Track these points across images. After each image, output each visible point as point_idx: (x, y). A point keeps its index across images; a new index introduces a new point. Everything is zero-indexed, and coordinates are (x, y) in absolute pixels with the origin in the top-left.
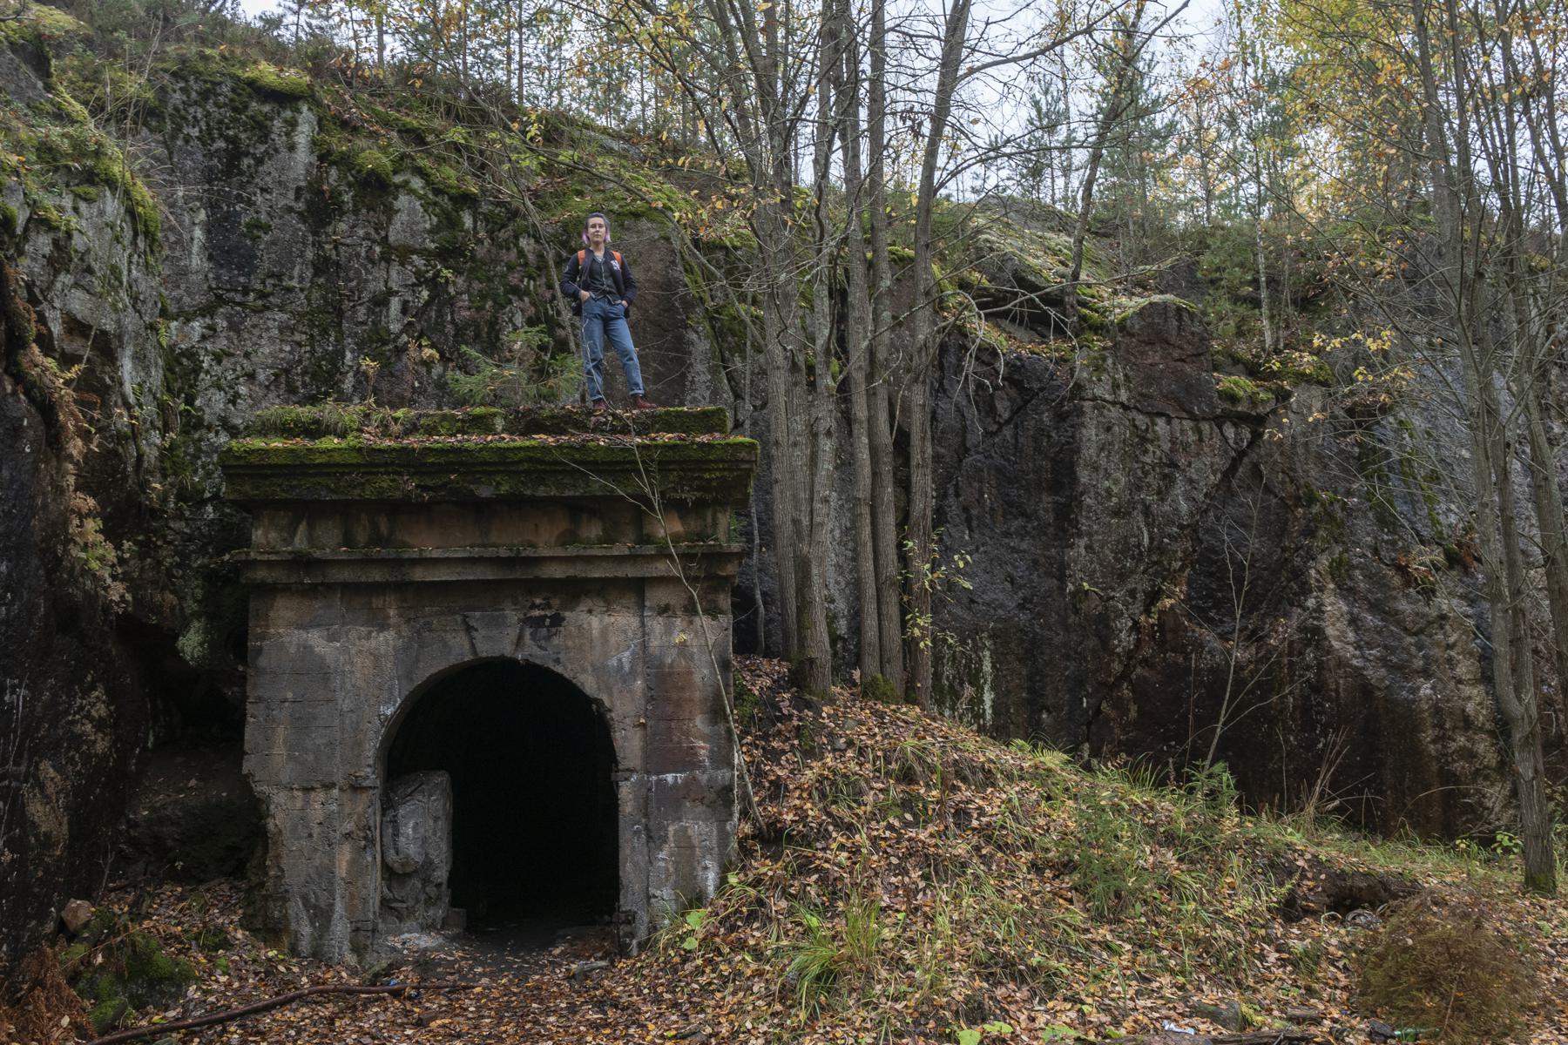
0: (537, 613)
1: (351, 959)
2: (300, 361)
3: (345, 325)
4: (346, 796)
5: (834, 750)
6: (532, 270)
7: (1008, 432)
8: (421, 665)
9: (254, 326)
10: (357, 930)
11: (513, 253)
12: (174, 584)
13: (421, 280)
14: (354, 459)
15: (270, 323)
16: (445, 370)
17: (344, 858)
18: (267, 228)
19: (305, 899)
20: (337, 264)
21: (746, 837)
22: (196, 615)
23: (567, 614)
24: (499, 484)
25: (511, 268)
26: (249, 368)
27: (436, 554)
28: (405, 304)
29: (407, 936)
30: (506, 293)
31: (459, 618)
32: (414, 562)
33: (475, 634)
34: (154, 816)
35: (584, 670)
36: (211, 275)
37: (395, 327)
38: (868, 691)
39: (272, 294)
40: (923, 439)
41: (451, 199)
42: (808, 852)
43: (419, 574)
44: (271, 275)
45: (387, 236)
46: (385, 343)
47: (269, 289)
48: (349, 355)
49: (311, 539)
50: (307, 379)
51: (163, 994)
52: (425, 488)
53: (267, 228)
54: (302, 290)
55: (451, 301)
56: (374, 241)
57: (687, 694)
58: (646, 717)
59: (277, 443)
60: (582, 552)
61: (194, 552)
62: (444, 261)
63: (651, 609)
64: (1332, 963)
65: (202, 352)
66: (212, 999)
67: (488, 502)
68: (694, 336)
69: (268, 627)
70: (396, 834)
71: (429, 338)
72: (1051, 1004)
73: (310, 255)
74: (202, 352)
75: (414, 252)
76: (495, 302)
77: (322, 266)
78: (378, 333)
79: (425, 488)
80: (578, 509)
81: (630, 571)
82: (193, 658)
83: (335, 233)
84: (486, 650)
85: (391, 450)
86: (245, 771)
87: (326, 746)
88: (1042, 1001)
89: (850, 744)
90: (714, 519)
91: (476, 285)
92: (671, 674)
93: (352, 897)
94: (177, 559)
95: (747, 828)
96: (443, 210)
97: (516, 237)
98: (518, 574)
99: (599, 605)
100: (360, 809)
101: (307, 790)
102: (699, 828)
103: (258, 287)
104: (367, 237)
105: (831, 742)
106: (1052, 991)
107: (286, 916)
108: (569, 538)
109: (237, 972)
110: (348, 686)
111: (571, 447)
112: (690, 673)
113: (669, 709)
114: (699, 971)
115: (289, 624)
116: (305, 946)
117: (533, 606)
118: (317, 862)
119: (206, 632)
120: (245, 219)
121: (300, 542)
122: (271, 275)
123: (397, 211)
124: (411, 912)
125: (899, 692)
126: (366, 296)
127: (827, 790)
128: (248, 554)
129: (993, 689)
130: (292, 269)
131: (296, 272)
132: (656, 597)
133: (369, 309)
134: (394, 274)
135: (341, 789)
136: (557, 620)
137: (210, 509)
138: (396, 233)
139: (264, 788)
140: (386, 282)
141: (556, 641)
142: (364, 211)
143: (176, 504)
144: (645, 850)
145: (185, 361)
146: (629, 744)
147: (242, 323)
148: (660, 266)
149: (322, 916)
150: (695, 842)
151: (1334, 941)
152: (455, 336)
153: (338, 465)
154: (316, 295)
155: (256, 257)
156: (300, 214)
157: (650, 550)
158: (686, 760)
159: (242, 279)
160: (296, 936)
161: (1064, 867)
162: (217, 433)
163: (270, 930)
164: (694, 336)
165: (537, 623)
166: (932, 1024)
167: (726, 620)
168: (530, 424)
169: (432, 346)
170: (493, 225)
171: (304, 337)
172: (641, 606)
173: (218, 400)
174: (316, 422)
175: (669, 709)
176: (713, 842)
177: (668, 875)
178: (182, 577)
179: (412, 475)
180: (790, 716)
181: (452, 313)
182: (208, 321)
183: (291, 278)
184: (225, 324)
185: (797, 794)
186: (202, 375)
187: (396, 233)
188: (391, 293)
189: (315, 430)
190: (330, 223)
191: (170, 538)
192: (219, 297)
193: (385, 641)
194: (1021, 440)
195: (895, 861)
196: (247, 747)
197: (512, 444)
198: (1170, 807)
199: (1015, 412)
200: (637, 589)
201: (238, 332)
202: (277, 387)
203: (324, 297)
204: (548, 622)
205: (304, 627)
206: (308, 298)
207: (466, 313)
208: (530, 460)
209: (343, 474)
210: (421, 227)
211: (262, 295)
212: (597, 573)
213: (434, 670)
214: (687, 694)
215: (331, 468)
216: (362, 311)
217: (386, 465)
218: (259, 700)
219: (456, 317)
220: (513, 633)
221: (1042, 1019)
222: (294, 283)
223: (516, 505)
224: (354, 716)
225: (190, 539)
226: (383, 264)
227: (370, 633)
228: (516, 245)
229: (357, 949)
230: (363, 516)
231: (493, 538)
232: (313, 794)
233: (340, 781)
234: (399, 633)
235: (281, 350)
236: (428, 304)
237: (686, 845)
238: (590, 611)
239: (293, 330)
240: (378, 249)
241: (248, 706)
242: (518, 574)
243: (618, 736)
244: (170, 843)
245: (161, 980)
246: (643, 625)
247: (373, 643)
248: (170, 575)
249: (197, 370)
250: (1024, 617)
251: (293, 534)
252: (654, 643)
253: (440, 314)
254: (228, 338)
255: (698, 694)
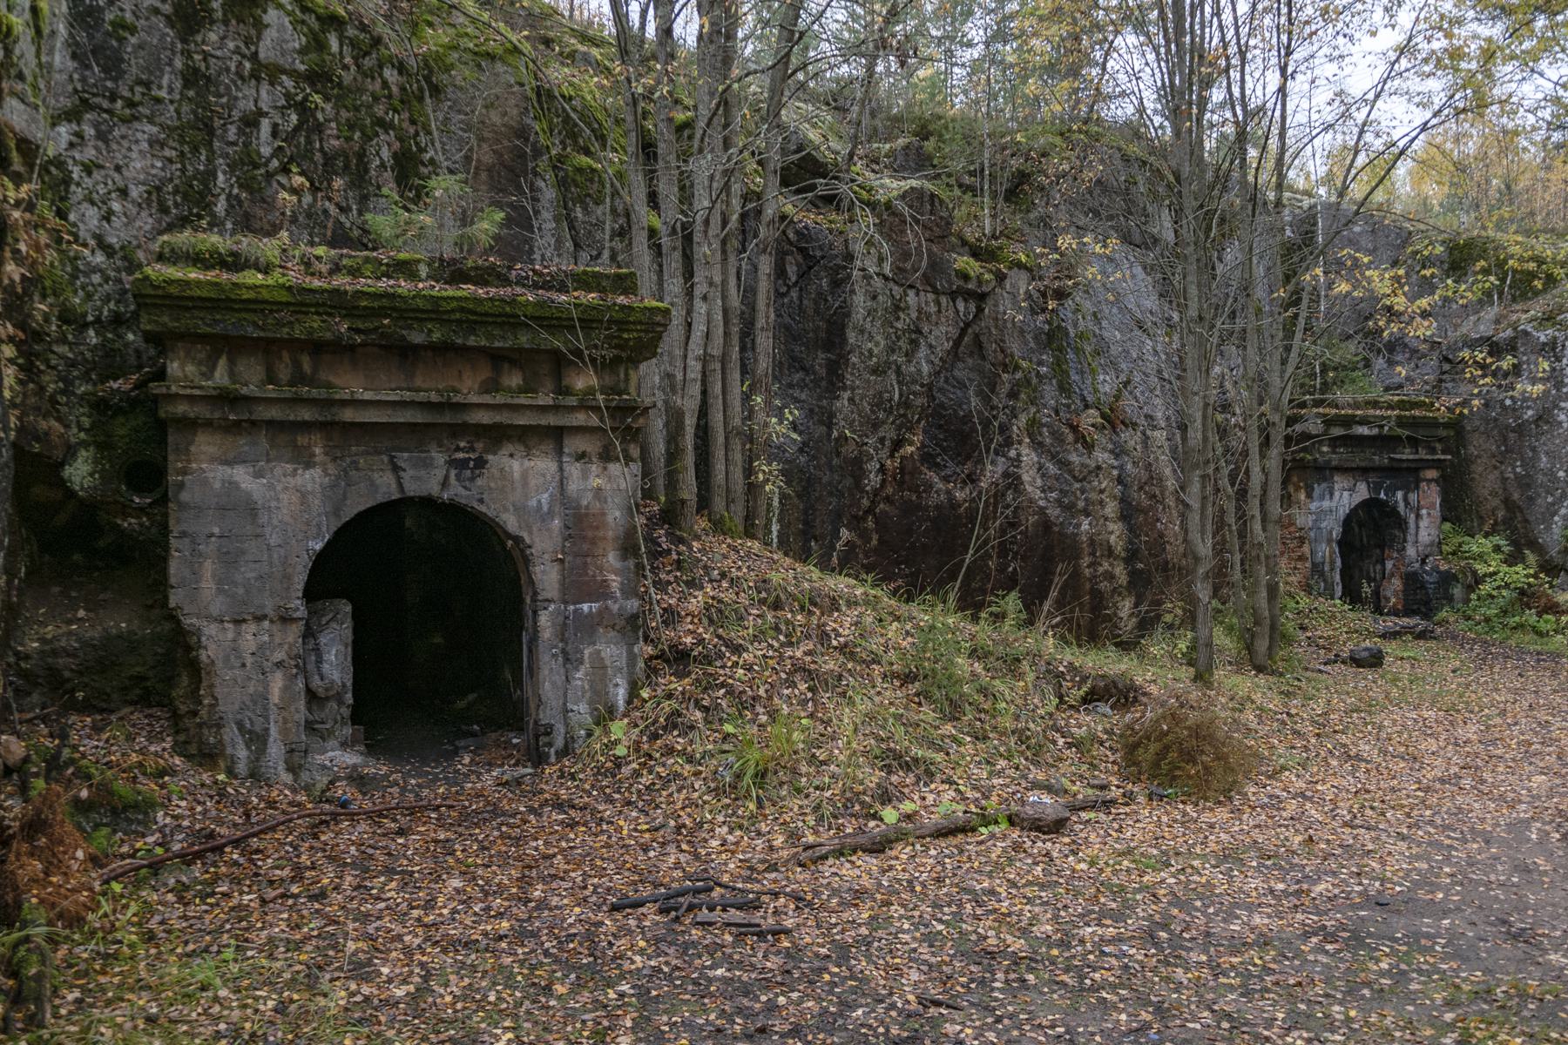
0: (461, 455)
1: (287, 778)
2: (171, 180)
3: (216, 144)
4: (275, 628)
5: (711, 581)
6: (396, 103)
7: (794, 294)
8: (348, 502)
9: (123, 137)
10: (292, 751)
11: (377, 86)
12: (58, 411)
13: (291, 102)
14: (284, 297)
15: (139, 135)
16: (315, 200)
17: (277, 682)
18: (133, 30)
19: (240, 726)
20: (208, 79)
21: (651, 658)
22: (84, 444)
23: (490, 457)
24: (430, 331)
25: (376, 99)
26: (121, 184)
27: (368, 396)
28: (275, 126)
29: (331, 754)
30: (373, 124)
31: (385, 459)
32: (344, 403)
33: (402, 474)
34: (47, 648)
35: (506, 510)
36: (76, 76)
37: (266, 151)
38: (719, 527)
39: (141, 103)
40: (768, 305)
41: (319, 18)
42: (711, 670)
43: (348, 415)
44: (140, 82)
45: (256, 53)
46: (256, 166)
47: (137, 98)
48: (221, 177)
49: (232, 374)
50: (179, 199)
51: (130, 821)
52: (358, 331)
53: (133, 30)
54: (172, 102)
55: (319, 128)
56: (244, 56)
57: (601, 534)
58: (563, 553)
59: (194, 275)
60: (509, 401)
61: (77, 378)
62: (312, 84)
63: (569, 455)
64: (1102, 743)
65: (70, 162)
66: (186, 823)
67: (417, 348)
68: (542, 184)
69: (189, 461)
70: (319, 661)
71: (299, 165)
72: (933, 786)
73: (178, 63)
74: (70, 162)
75: (284, 72)
76: (363, 133)
77: (192, 77)
78: (249, 155)
79: (358, 331)
80: (499, 359)
81: (552, 420)
82: (82, 488)
83: (204, 42)
84: (413, 489)
85: (323, 291)
86: (172, 604)
87: (256, 579)
88: (926, 785)
89: (723, 575)
90: (627, 375)
91: (344, 114)
92: (587, 515)
93: (285, 721)
94: (61, 385)
95: (650, 650)
96: (311, 30)
97: (381, 67)
98: (447, 418)
99: (519, 449)
100: (290, 639)
101: (238, 622)
102: (611, 650)
103: (126, 94)
104: (237, 51)
105: (707, 574)
106: (931, 775)
107: (221, 742)
108: (492, 386)
109: (189, 793)
110: (275, 522)
111: (502, 300)
112: (604, 514)
113: (585, 547)
114: (637, 774)
115: (212, 460)
116: (242, 768)
117: (458, 449)
118: (251, 690)
119: (96, 462)
120: (109, 16)
121: (221, 376)
122: (140, 82)
123: (267, 26)
124: (330, 732)
125: (741, 528)
126: (236, 114)
127: (715, 614)
128: (168, 388)
129: (779, 521)
130: (161, 77)
131: (165, 82)
132: (573, 444)
133: (239, 128)
134: (263, 93)
135: (272, 621)
136: (481, 463)
137: (92, 333)
138: (266, 50)
139: (194, 621)
140: (256, 101)
141: (479, 482)
142: (234, 22)
143: (59, 327)
144: (562, 671)
145: (53, 169)
146: (547, 577)
147: (110, 132)
148: (515, 112)
149: (257, 740)
150: (608, 663)
151: (1100, 728)
152: (325, 165)
153: (266, 302)
154: (185, 108)
155: (122, 60)
156: (167, 17)
157: (572, 401)
158: (599, 592)
159: (109, 84)
160: (233, 760)
161: (907, 678)
162: (93, 252)
163: (207, 756)
164: (542, 184)
165: (462, 465)
166: (857, 807)
167: (636, 468)
168: (457, 275)
169: (301, 174)
170: (360, 52)
171: (174, 153)
172: (559, 452)
173: (92, 214)
174: (234, 254)
175: (585, 547)
176: (623, 662)
177: (584, 692)
178: (67, 404)
179: (343, 317)
180: (670, 550)
181: (321, 141)
182: (75, 127)
183: (160, 87)
184: (92, 132)
185: (689, 619)
186: (73, 188)
187: (266, 50)
188: (261, 113)
189: (235, 262)
190: (198, 31)
191: (53, 362)
192: (84, 101)
193: (312, 478)
194: (805, 302)
195: (783, 676)
196: (173, 581)
197: (444, 294)
198: (983, 631)
199: (801, 276)
200: (557, 435)
201: (106, 142)
202: (149, 206)
203: (194, 112)
204: (472, 464)
205: (229, 463)
206: (177, 111)
207: (335, 143)
208: (462, 310)
209: (271, 311)
210: (290, 45)
211: (131, 104)
212: (522, 420)
213: (362, 508)
214: (601, 534)
215: (257, 305)
216: (232, 130)
217: (317, 305)
218: (183, 534)
219: (325, 145)
220: (439, 473)
221: (930, 798)
222: (163, 94)
223: (444, 352)
224: (282, 551)
225: (72, 364)
226: (253, 82)
227: (295, 470)
228: (381, 75)
229: (292, 769)
230: (285, 354)
231: (418, 382)
232: (244, 626)
233: (271, 613)
234: (325, 471)
235: (153, 166)
236: (297, 129)
237: (600, 666)
238: (511, 455)
239: (163, 145)
240: (248, 65)
241: (172, 541)
242: (447, 418)
243: (537, 570)
244: (67, 674)
245: (125, 808)
246: (561, 469)
247: (299, 480)
248: (53, 401)
249: (67, 181)
250: (803, 459)
251: (213, 368)
252: (573, 487)
253: (309, 142)
254: (96, 148)
255: (610, 533)
